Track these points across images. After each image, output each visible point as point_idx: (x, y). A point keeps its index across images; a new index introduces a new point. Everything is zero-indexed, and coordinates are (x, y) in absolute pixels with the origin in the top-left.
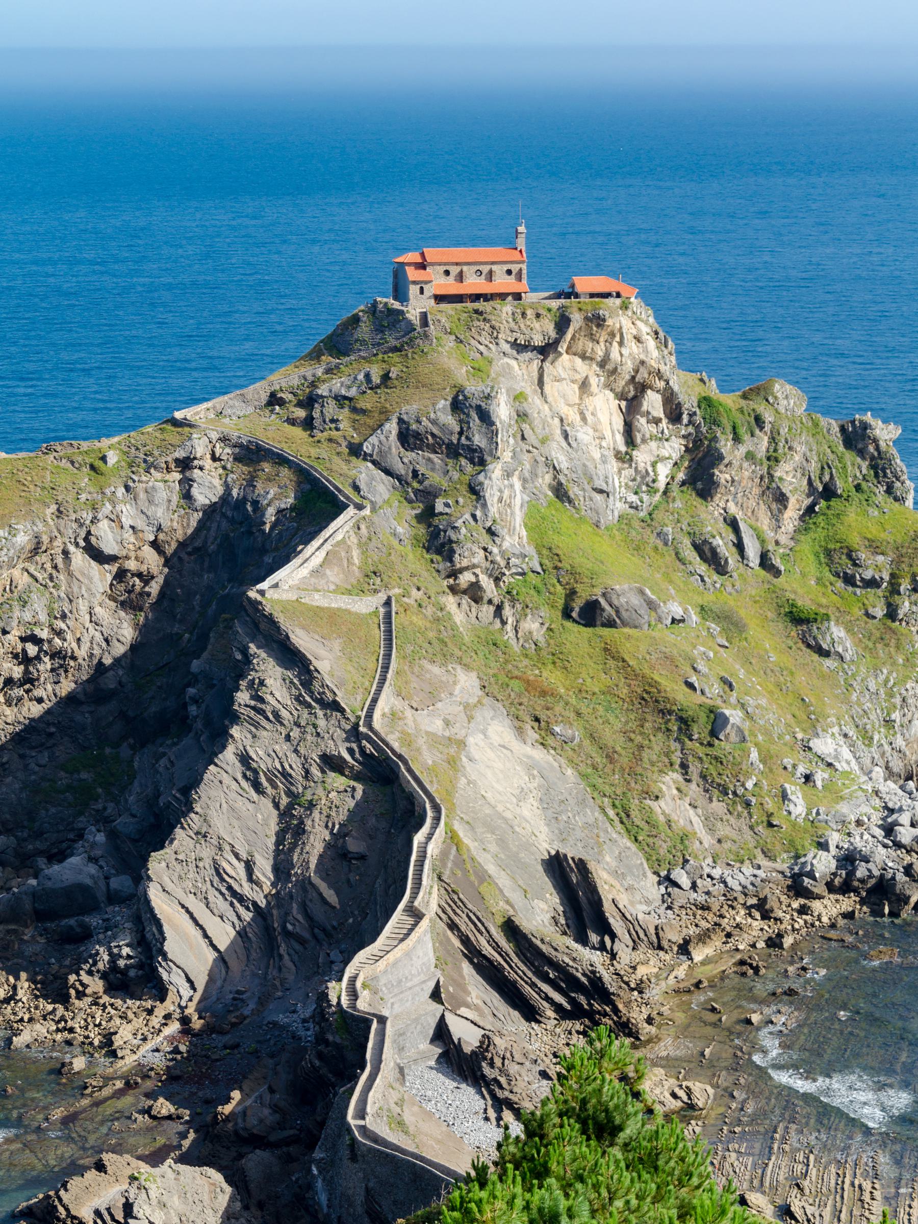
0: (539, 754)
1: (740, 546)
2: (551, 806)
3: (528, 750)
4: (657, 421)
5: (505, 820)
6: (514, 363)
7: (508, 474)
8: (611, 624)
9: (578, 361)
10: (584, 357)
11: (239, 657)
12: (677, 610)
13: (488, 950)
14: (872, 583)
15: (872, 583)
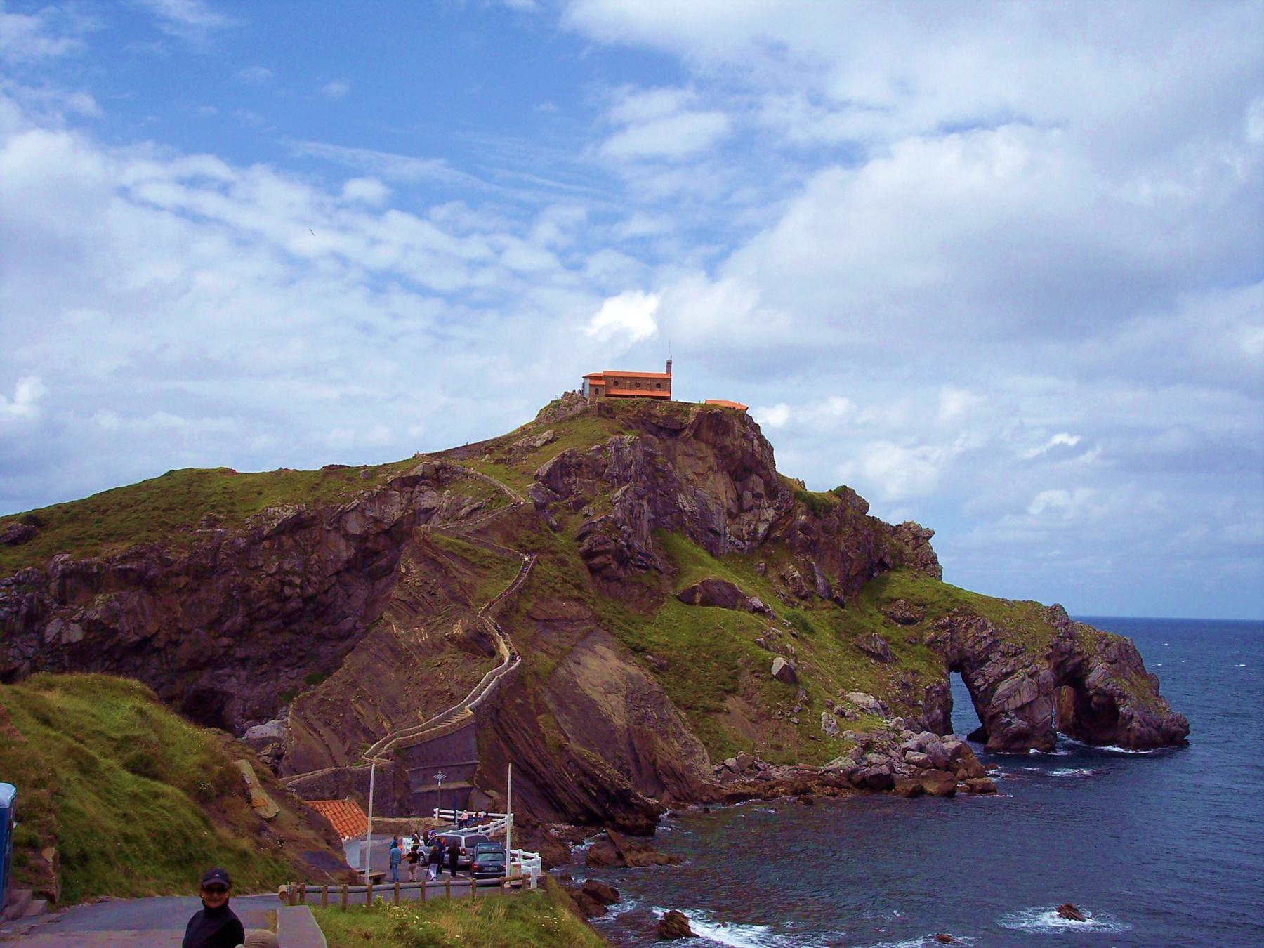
0: (632, 670)
1: (813, 582)
2: (635, 697)
3: (623, 665)
4: (759, 496)
5: (591, 701)
6: (655, 439)
7: (640, 497)
8: (706, 602)
9: (703, 446)
10: (707, 443)
11: (403, 570)
12: (758, 603)
13: (534, 760)
14: (909, 621)
15: (909, 621)
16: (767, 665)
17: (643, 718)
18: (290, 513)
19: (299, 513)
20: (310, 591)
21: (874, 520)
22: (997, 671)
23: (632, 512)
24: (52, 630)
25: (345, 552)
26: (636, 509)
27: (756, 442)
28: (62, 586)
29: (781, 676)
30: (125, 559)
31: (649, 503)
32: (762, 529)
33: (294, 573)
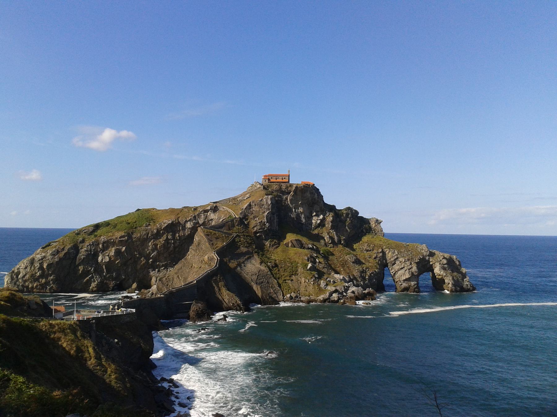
0: (263, 268)
16: (306, 265)
17: (262, 282)
18: (170, 222)
19: (173, 222)
20: (176, 245)
21: (362, 217)
22: (398, 267)
23: (270, 219)
24: (100, 259)
25: (187, 232)
26: (272, 218)
27: (316, 195)
28: (103, 245)
29: (310, 269)
30: (120, 238)
31: (277, 215)
32: (319, 222)
33: (172, 240)
